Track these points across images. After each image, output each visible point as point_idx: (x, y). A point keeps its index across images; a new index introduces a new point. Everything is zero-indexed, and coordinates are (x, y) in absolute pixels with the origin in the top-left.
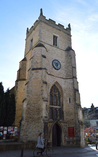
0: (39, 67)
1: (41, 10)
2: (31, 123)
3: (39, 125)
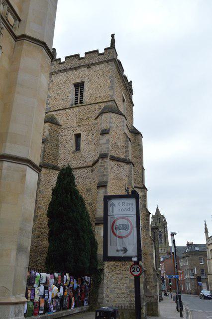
0: (122, 156)
1: (113, 36)
2: (113, 270)
3: (127, 276)
